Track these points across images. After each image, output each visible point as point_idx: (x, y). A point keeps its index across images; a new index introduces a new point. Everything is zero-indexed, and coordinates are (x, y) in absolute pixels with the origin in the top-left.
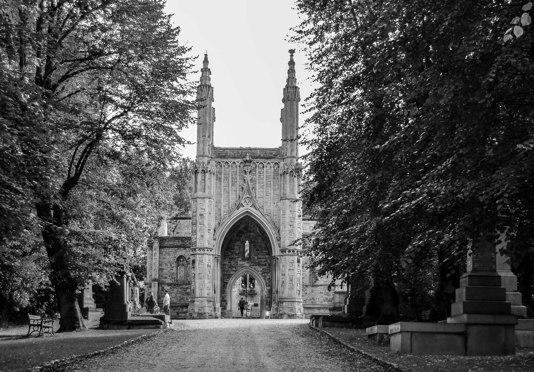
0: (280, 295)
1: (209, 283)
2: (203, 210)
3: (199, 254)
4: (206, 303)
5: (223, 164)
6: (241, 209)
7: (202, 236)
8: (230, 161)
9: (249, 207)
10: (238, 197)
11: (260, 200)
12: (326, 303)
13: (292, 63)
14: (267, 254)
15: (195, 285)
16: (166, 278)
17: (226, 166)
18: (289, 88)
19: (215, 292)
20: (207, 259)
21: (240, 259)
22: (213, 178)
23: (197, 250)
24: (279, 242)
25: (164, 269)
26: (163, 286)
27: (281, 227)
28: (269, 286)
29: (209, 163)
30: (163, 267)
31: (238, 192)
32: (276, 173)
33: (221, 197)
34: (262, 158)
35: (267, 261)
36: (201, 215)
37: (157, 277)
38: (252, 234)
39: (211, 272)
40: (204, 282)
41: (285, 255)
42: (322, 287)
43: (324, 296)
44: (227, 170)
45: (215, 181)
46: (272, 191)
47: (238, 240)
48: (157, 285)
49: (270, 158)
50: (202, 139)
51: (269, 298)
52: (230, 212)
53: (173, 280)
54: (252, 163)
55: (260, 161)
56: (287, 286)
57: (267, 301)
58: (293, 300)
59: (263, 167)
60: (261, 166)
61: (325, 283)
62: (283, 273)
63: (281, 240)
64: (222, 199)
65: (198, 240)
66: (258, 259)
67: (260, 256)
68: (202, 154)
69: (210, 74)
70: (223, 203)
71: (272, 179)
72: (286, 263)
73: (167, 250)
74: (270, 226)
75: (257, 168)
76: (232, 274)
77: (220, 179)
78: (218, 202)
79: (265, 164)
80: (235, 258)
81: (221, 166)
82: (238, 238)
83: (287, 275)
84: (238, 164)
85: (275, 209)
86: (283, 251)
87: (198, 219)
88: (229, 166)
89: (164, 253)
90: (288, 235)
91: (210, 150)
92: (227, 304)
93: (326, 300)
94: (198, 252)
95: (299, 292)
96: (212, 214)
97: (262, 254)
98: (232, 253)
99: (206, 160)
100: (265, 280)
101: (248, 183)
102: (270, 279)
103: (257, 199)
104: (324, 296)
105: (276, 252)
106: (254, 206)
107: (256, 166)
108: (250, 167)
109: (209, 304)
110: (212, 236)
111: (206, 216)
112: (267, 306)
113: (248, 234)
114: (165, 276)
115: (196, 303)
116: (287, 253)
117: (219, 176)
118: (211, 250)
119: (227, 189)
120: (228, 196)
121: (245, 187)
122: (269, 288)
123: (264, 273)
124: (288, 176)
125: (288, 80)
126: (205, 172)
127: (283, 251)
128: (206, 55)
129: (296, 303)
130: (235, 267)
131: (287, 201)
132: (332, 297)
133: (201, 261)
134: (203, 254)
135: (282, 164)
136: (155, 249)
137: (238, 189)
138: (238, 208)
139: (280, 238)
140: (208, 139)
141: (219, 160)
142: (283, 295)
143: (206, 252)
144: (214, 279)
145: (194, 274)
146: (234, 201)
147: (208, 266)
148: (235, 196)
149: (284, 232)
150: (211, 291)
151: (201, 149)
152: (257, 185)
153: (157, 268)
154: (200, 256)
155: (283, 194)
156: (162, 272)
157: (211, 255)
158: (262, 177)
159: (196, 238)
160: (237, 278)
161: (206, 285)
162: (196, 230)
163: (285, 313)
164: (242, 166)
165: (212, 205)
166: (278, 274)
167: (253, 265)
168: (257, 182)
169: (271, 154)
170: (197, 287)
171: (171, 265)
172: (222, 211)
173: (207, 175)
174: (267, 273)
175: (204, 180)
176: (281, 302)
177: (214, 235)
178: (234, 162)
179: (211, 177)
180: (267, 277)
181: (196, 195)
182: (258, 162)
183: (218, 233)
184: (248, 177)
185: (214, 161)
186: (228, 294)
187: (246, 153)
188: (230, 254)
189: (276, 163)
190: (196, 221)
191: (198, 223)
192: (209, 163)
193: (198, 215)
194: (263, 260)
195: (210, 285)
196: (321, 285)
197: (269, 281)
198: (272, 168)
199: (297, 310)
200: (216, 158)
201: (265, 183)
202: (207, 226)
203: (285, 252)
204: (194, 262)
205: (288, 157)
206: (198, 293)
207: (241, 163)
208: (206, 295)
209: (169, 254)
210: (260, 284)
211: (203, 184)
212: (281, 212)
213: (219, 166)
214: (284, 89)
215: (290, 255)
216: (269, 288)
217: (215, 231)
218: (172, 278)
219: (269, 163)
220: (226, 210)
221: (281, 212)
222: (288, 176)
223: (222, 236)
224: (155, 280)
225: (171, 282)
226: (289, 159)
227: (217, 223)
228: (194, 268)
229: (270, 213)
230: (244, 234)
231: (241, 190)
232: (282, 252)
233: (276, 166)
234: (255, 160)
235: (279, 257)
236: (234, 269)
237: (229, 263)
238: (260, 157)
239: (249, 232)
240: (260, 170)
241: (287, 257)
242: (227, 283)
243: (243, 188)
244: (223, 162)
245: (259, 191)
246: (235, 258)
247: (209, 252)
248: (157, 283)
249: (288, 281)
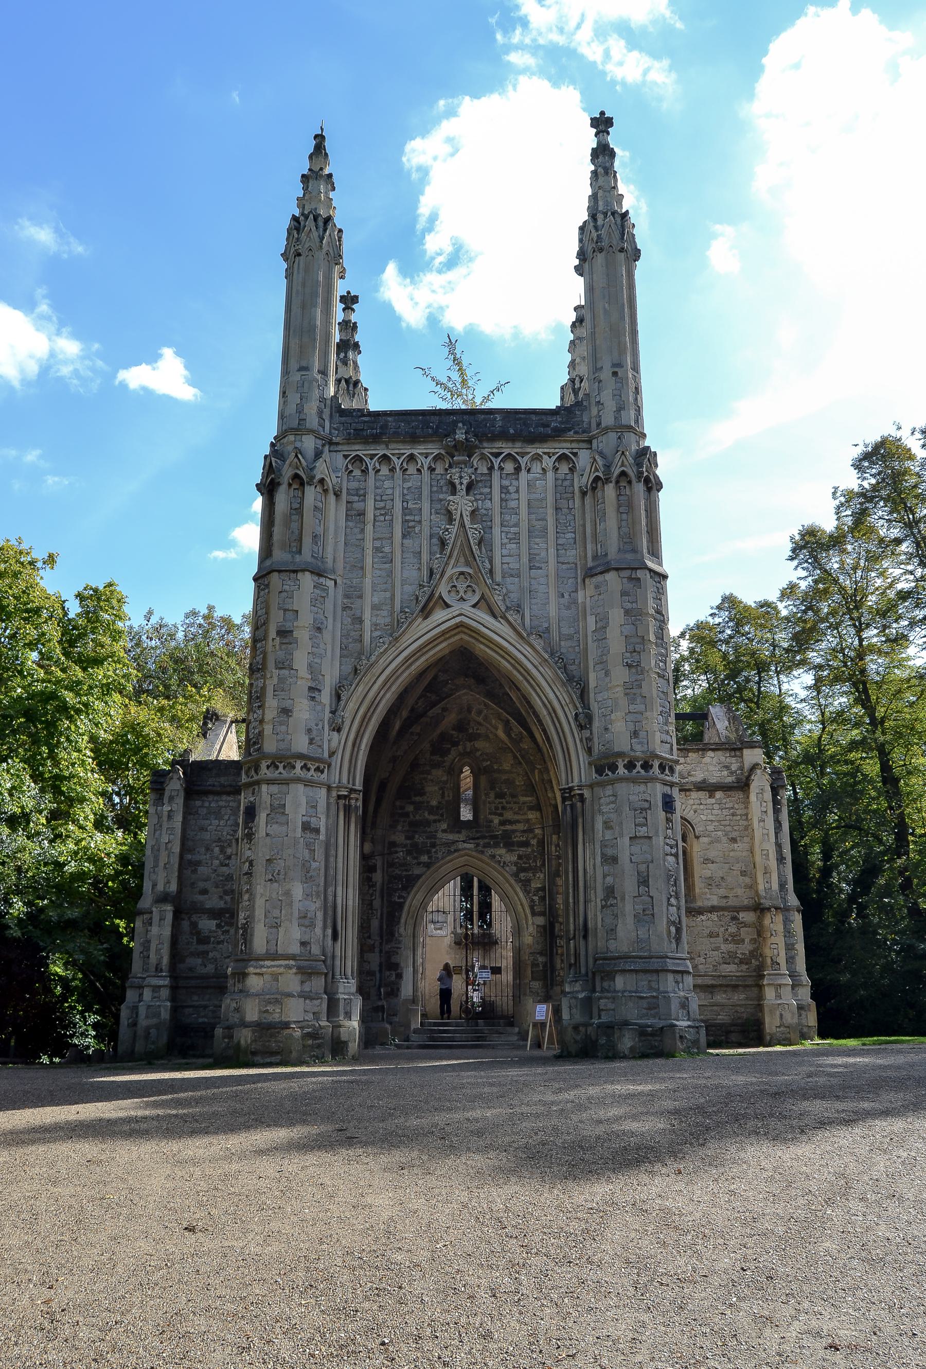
0: (598, 942)
1: (307, 895)
2: (290, 615)
3: (270, 782)
4: (291, 982)
5: (371, 464)
6: (440, 615)
7: (286, 712)
8: (399, 451)
9: (466, 607)
10: (425, 573)
11: (511, 584)
12: (730, 969)
13: (603, 154)
14: (531, 808)
15: (252, 908)
16: (204, 892)
17: (385, 470)
18: (600, 217)
19: (335, 937)
20: (304, 800)
21: (444, 826)
22: (335, 512)
23: (264, 765)
24: (586, 733)
25: (198, 863)
26: (194, 918)
27: (592, 677)
28: (542, 914)
29: (318, 454)
30: (196, 857)
31: (425, 557)
32: (562, 490)
33: (364, 576)
34: (512, 439)
35: (531, 830)
36: (283, 633)
37: (173, 887)
38: (480, 744)
39: (320, 854)
40: (288, 893)
41: (612, 782)
42: (714, 916)
43: (724, 947)
44: (387, 484)
45: (342, 522)
46: (552, 551)
47: (437, 765)
48: (169, 917)
49: (541, 439)
50: (296, 377)
51: (541, 954)
52: (394, 631)
53: (228, 898)
54: (475, 460)
55: (507, 448)
56: (629, 908)
57: (534, 965)
58: (655, 964)
59: (518, 469)
60: (509, 467)
61: (723, 903)
62: (610, 852)
63: (596, 724)
64: (368, 581)
65: (268, 729)
66: (502, 823)
67: (508, 815)
68: (295, 424)
69: (334, 189)
70: (369, 599)
71: (550, 511)
72: (618, 811)
73: (212, 802)
74: (549, 673)
75: (496, 475)
76: (419, 877)
77: (362, 514)
78: (353, 594)
79: (523, 461)
80: (428, 823)
81: (365, 472)
82: (437, 758)
83: (624, 858)
84: (426, 462)
85: (566, 613)
86: (604, 765)
87: (269, 648)
88: (392, 470)
89: (203, 811)
90: (623, 702)
91: (326, 415)
92: (400, 976)
93: (730, 958)
94: (265, 772)
95: (679, 930)
96: (327, 636)
97: (516, 807)
98: (418, 806)
99: (309, 444)
100: (527, 892)
101: (463, 525)
102: (543, 889)
103: (498, 578)
104: (724, 947)
105: (576, 771)
106: (483, 603)
107: (491, 468)
108: (470, 471)
109: (307, 987)
110: (327, 715)
111: (303, 635)
112: (536, 985)
113: (468, 745)
114: (201, 885)
115: (254, 983)
116: (621, 771)
117: (358, 506)
118: (323, 765)
119: (387, 549)
120: (390, 573)
121: (451, 538)
122: (540, 920)
123: (524, 870)
124: (610, 491)
125: (594, 198)
127: (604, 765)
128: (320, 139)
129: (670, 977)
130: (429, 852)
131: (611, 576)
132: (751, 947)
133: (278, 810)
134: (286, 782)
135: (584, 458)
136: (171, 799)
137: (425, 543)
138: (426, 612)
139: (589, 718)
140: (319, 377)
141: (361, 450)
142: (612, 945)
144: (329, 880)
145: (251, 864)
146: (409, 589)
147: (306, 827)
148: (415, 574)
149: (605, 695)
150: (318, 930)
151: (292, 408)
152: (497, 530)
153: (175, 861)
154: (274, 789)
155: (595, 557)
156: (195, 871)
157: (321, 784)
158: (513, 504)
159: (261, 721)
160: (434, 889)
161: (296, 906)
162: (264, 688)
163: (626, 1023)
164: (439, 470)
165: (329, 605)
166: (589, 859)
167: (487, 846)
168: (497, 520)
169: (546, 426)
170: (259, 913)
171: (222, 850)
172: (367, 624)
173: (311, 493)
174: (535, 870)
175: (299, 511)
176: (601, 971)
177: (333, 712)
178: (412, 458)
180: (536, 884)
181: (268, 563)
182: (497, 455)
183: (352, 706)
184: (462, 504)
185: (340, 456)
186: (407, 942)
187: (455, 423)
188: (410, 808)
189: (563, 458)
190: (264, 658)
191: (271, 664)
192: (318, 454)
193: (272, 633)
194: (520, 827)
195: (315, 907)
196: (713, 909)
197: (543, 899)
198: (550, 475)
199: (675, 1005)
200: (349, 440)
201: (524, 525)
202: (303, 672)
203: (613, 768)
204: (251, 813)
205: (607, 430)
206: (259, 944)
207: (437, 458)
208: (295, 949)
209: (218, 815)
210: (510, 907)
211: (295, 526)
212: (591, 620)
213: (357, 473)
214: (582, 229)
215: (634, 781)
216: (540, 920)
217: (339, 697)
218: (226, 893)
219: (537, 458)
220: (381, 621)
221: (591, 620)
222: (610, 491)
223: (365, 720)
224: (163, 898)
225: (221, 904)
226: (613, 436)
227: (348, 668)
228: (249, 836)
229: (548, 630)
230: (456, 744)
231: (436, 549)
232: (600, 771)
233: (564, 468)
234: (488, 449)
235: (587, 793)
236: (424, 858)
237: (407, 838)
238: (503, 436)
239: (473, 737)
240: (506, 483)
241: (623, 789)
242: (401, 906)
243: (443, 543)
244: (372, 457)
245: (503, 554)
246: (428, 823)
247: (316, 776)
248: (169, 908)
249: (629, 885)
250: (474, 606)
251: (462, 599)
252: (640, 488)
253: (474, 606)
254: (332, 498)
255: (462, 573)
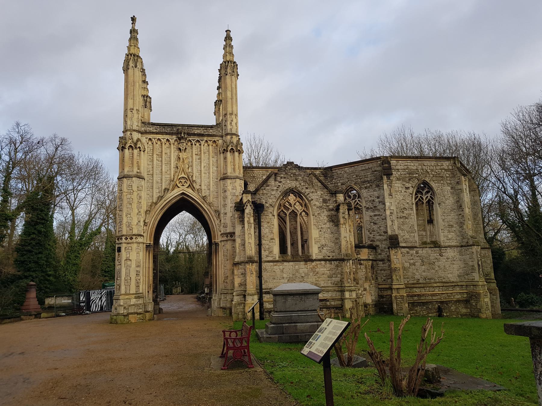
9: (184, 188)
55: (197, 138)
125: (225, 56)
126: (133, 149)
143: (134, 240)
179: (140, 154)
184: (183, 155)
250: (188, 187)
251: (183, 185)
252: (236, 154)
253: (188, 187)
254: (142, 152)
255: (183, 177)
